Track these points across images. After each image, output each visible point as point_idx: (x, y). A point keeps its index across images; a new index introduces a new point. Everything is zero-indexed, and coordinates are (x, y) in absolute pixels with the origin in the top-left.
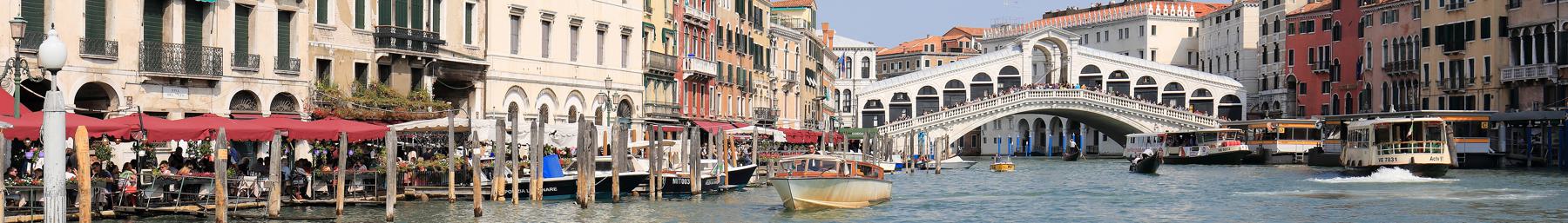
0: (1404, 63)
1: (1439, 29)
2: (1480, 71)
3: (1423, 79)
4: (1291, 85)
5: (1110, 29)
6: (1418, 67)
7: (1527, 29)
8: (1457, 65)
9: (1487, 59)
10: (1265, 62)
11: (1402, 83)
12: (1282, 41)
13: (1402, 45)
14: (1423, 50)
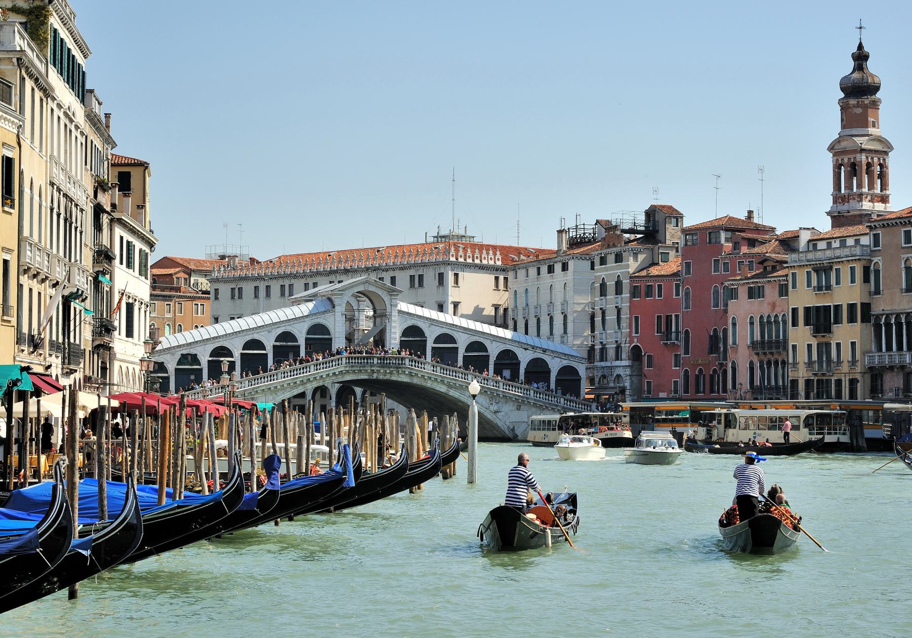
0: (770, 342)
2: (846, 355)
3: (791, 361)
4: (636, 354)
5: (399, 275)
6: (786, 349)
7: (888, 316)
8: (824, 348)
9: (853, 344)
11: (769, 363)
12: (625, 306)
13: (769, 322)
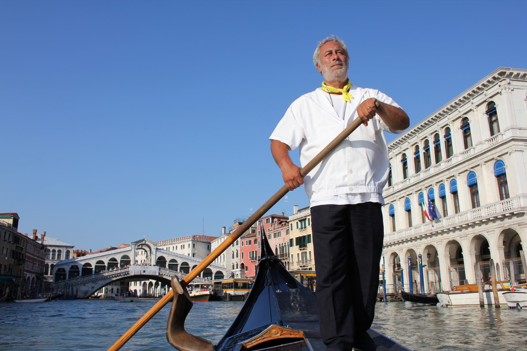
1: (297, 239)
6: (289, 256)
10: (233, 258)
14: (290, 248)
